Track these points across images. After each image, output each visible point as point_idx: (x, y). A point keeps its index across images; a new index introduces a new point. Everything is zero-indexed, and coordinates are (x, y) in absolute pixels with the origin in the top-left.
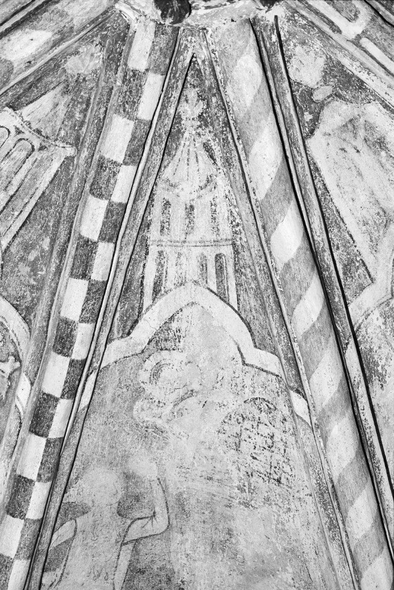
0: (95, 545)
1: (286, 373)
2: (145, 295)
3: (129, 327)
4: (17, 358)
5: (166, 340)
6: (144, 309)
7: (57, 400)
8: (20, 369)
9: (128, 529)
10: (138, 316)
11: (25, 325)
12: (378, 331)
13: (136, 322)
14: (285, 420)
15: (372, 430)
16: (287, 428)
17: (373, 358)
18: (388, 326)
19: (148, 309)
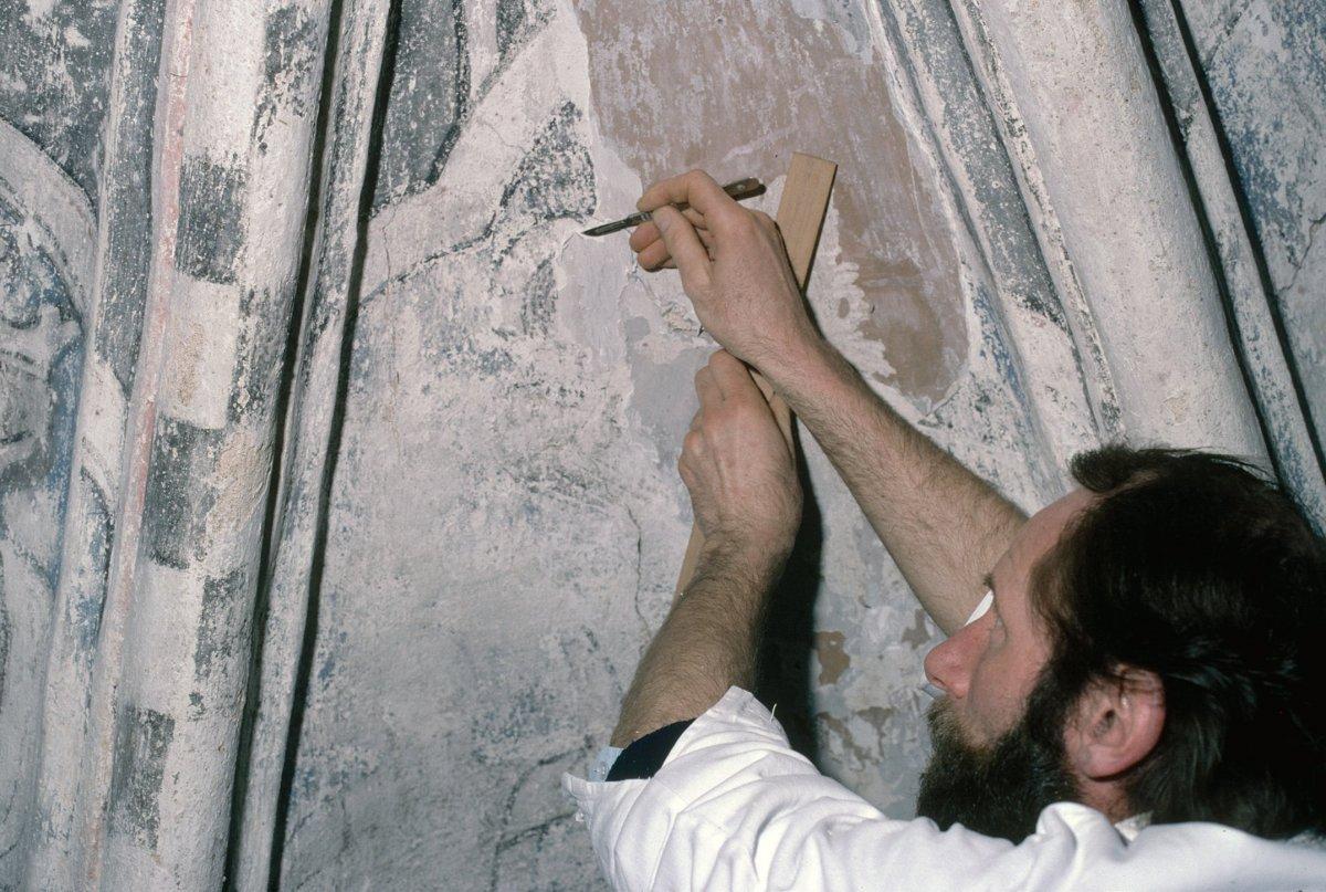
0: (417, 863)
1: (986, 244)
2: (472, 36)
3: (430, 154)
4: (69, 309)
5: (562, 182)
6: (475, 86)
7: (217, 437)
8: (79, 345)
9: (512, 800)
10: (458, 114)
11: (76, 193)
12: (1271, 67)
13: (453, 132)
14: (986, 399)
15: (1286, 401)
16: (995, 427)
17: (1259, 163)
18: (1300, 52)
19: (487, 84)
